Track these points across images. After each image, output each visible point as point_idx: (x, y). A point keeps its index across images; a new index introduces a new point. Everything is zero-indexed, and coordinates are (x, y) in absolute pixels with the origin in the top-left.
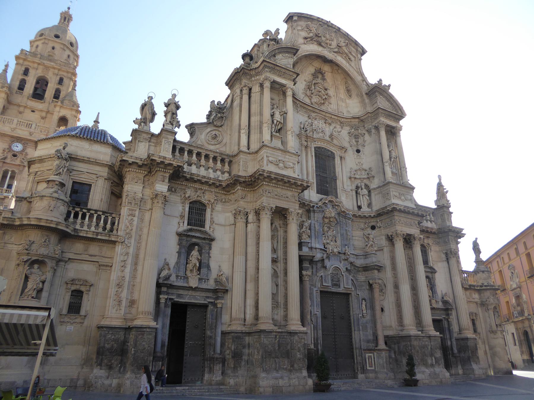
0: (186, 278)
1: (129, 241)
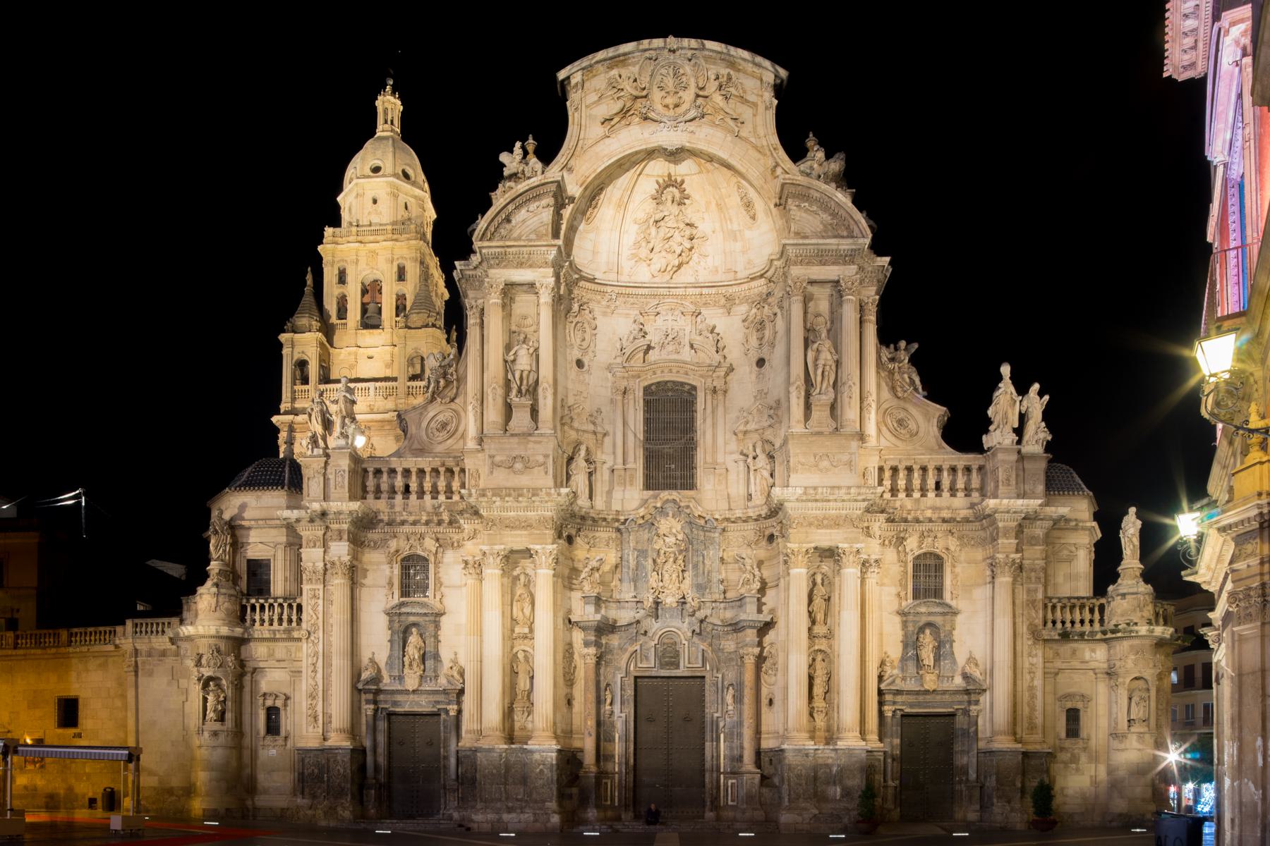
0: (401, 678)
1: (316, 635)
